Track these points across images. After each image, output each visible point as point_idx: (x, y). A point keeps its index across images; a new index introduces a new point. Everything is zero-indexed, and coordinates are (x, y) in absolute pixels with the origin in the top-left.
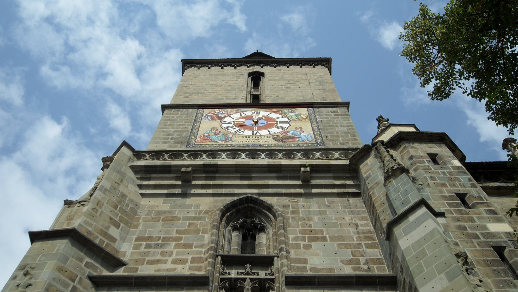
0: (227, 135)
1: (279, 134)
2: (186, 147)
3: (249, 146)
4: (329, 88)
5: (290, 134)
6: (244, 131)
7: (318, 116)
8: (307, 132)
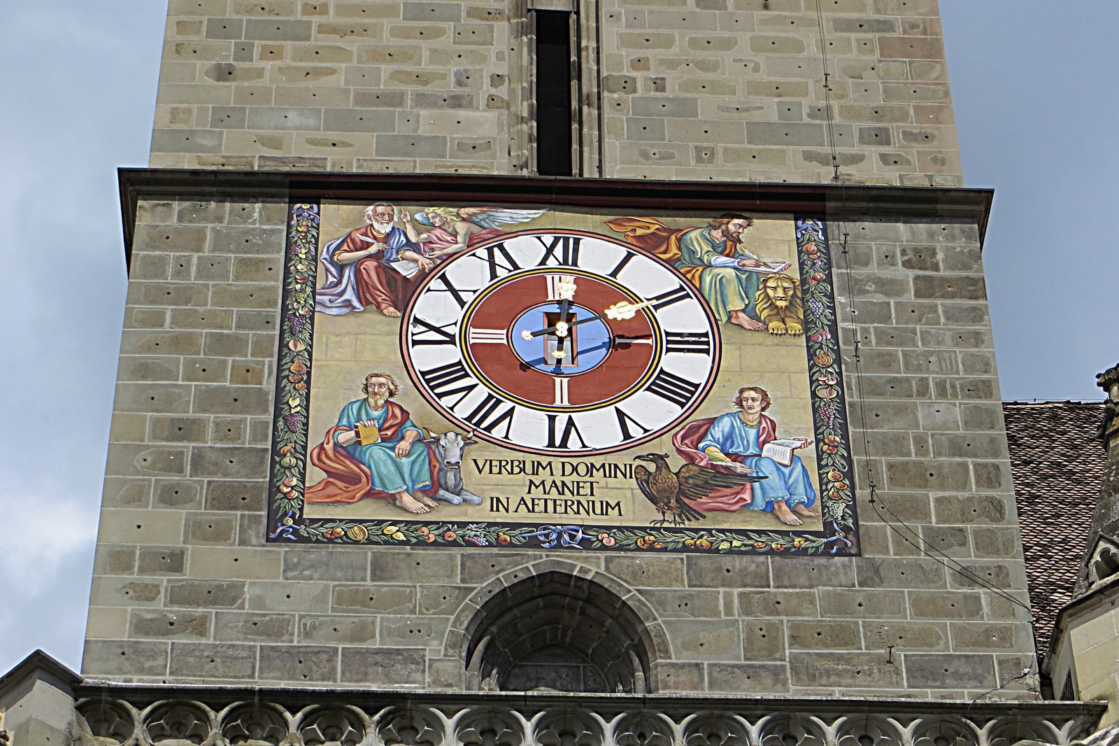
0: (437, 440)
1: (665, 446)
3: (534, 543)
4: (911, 16)
5: (713, 453)
6: (510, 412)
8: (787, 433)
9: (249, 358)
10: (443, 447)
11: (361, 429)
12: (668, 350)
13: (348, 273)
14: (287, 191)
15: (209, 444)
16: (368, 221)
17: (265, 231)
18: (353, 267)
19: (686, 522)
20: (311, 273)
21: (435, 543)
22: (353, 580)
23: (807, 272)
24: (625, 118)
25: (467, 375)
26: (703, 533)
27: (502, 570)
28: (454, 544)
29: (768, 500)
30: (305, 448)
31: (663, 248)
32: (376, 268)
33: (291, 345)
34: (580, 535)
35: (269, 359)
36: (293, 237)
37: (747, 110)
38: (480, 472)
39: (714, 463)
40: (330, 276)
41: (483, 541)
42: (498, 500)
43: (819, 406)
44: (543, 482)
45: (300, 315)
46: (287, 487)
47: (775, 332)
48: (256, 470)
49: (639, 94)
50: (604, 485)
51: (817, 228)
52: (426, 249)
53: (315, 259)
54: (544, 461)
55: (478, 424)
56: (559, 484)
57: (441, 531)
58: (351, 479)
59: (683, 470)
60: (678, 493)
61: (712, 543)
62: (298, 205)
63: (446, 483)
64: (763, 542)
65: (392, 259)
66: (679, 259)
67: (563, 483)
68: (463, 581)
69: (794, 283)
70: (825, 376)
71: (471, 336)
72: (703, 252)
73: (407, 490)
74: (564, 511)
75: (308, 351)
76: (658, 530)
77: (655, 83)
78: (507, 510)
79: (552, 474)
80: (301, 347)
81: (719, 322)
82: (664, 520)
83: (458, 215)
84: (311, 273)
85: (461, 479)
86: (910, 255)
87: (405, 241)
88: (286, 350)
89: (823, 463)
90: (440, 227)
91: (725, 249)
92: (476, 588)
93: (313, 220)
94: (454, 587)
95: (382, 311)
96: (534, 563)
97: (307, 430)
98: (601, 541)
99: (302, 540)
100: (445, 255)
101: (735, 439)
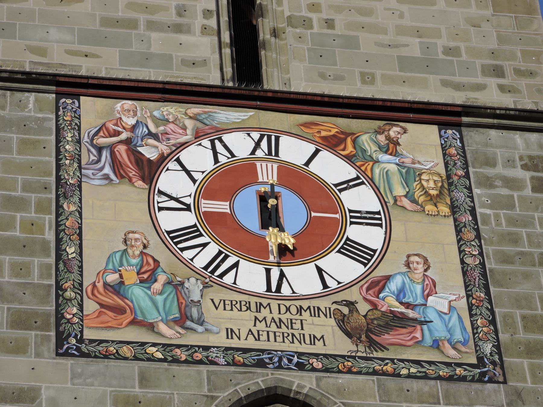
0: (182, 284)
1: (353, 295)
2: (58, 354)
3: (261, 364)
6: (236, 265)
7: (480, 185)
9: (33, 215)
10: (187, 288)
11: (123, 272)
12: (351, 223)
13: (105, 154)
14: (54, 88)
15: (7, 279)
16: (118, 115)
17: (39, 119)
18: (109, 149)
19: (375, 353)
20: (77, 152)
21: (186, 362)
22: (125, 387)
23: (451, 169)
24: (306, 47)
25: (201, 235)
26: (387, 361)
27: (238, 384)
28: (200, 362)
29: (434, 338)
30: (81, 285)
31: (342, 147)
32: (127, 151)
33: (65, 206)
34: (295, 359)
35: (49, 216)
36: (61, 124)
37: (396, 46)
38: (217, 308)
39: (392, 309)
40: (91, 156)
41: (222, 361)
42: (232, 330)
43: (467, 270)
44: (265, 318)
45: (70, 184)
46: (70, 314)
47: (430, 213)
48: (44, 300)
49: (316, 30)
50: (311, 323)
51: (455, 137)
52: (164, 138)
53: (79, 142)
54: (265, 302)
55: (213, 272)
56: (277, 320)
57: (190, 352)
58: (119, 311)
59: (369, 313)
60: (366, 330)
61: (395, 369)
62: (63, 100)
63: (191, 316)
64: (433, 370)
65: (138, 145)
66: (354, 156)
67: (280, 320)
68: (209, 390)
69: (441, 177)
70: (470, 248)
71: (203, 205)
72: (372, 152)
73: (162, 320)
74: (282, 340)
75: (79, 212)
76: (354, 357)
77: (326, 23)
78: (239, 338)
79: (271, 313)
80: (73, 208)
81: (388, 204)
82: (358, 351)
83: (186, 114)
84: (77, 152)
85: (202, 313)
86: (526, 161)
87: (147, 131)
88: (61, 210)
89: (474, 312)
90: (173, 122)
91: (388, 150)
92: (220, 396)
93: (75, 112)
94: (203, 395)
95: (133, 183)
96: (263, 379)
97: (82, 271)
98: (312, 364)
99: (83, 355)
100: (179, 143)
101: (405, 291)
